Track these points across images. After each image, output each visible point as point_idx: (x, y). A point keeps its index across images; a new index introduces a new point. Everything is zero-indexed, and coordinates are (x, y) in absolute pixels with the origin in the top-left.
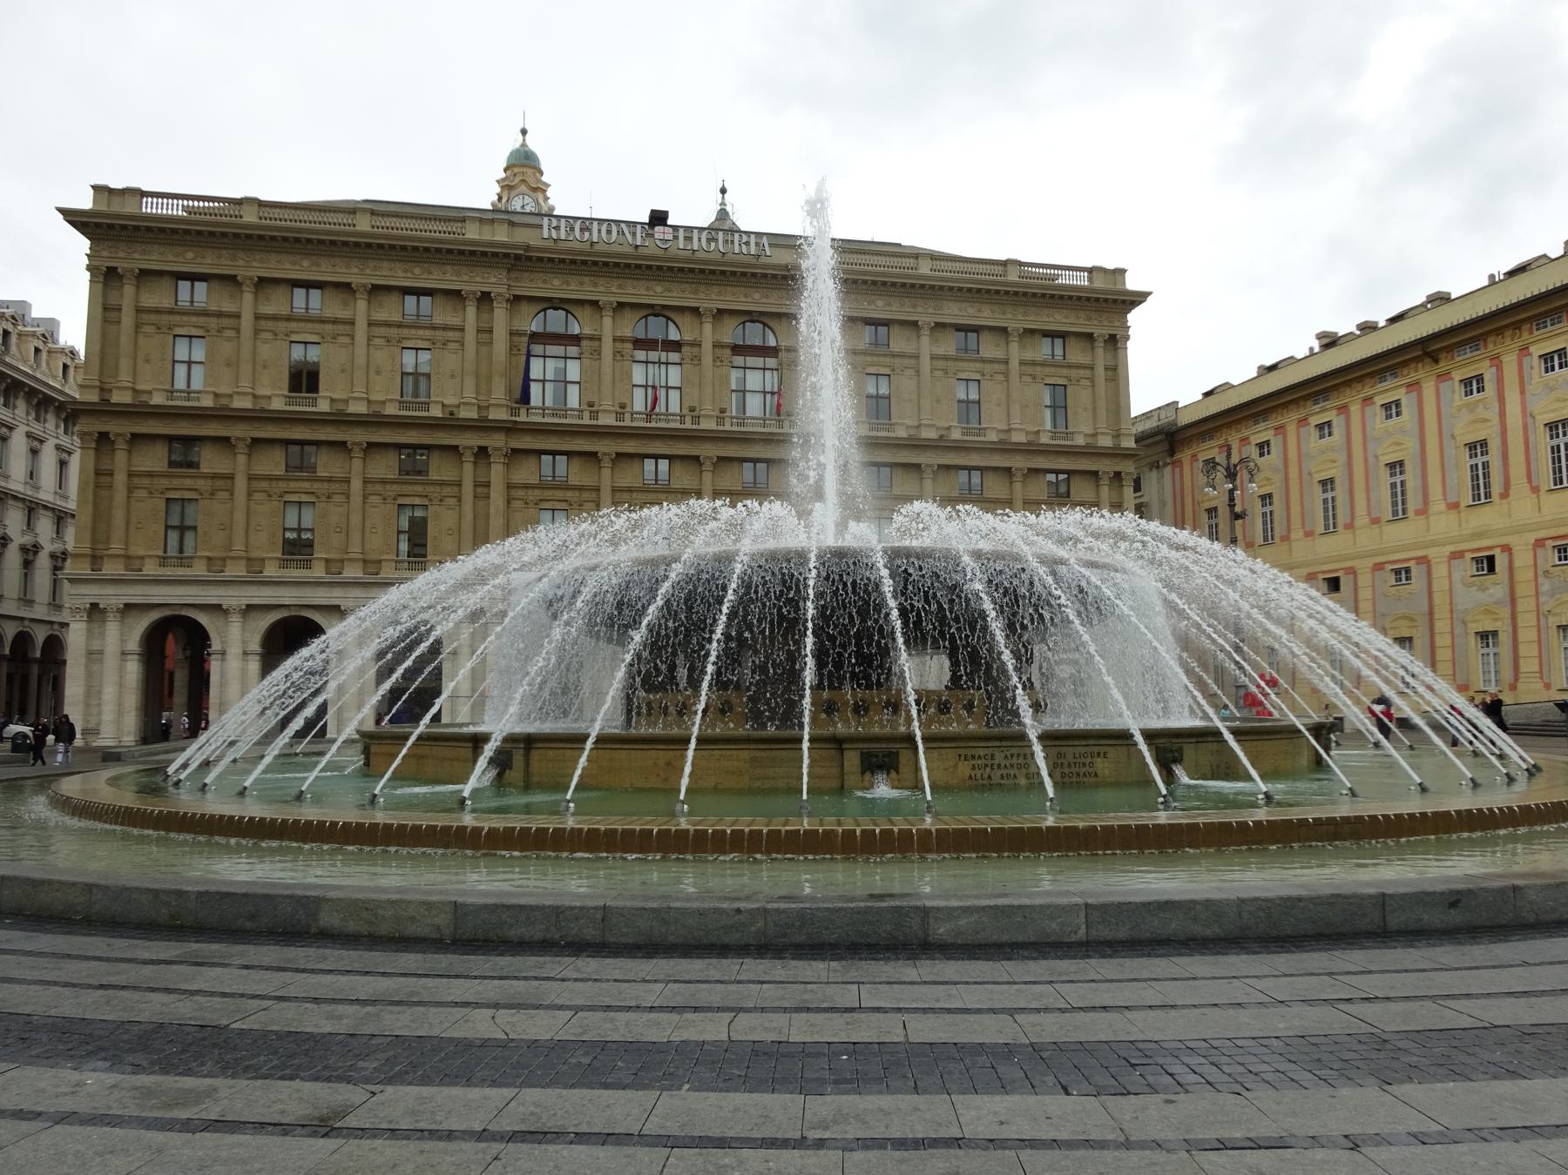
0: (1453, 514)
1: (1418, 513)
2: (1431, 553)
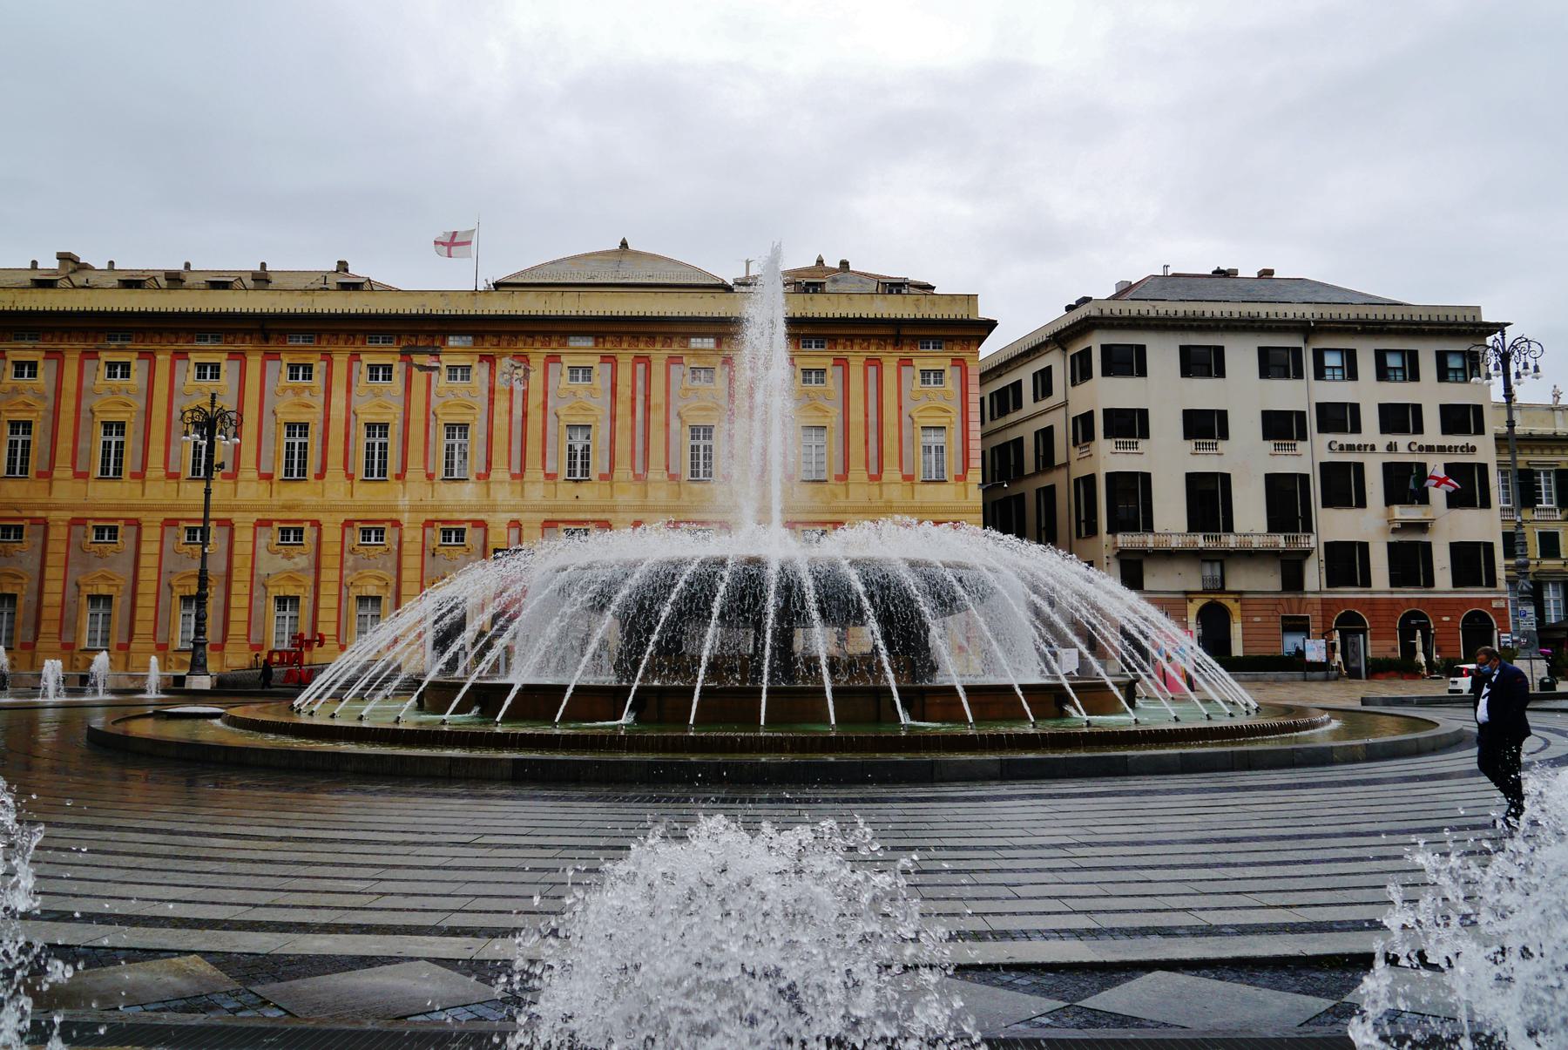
2: (236, 517)
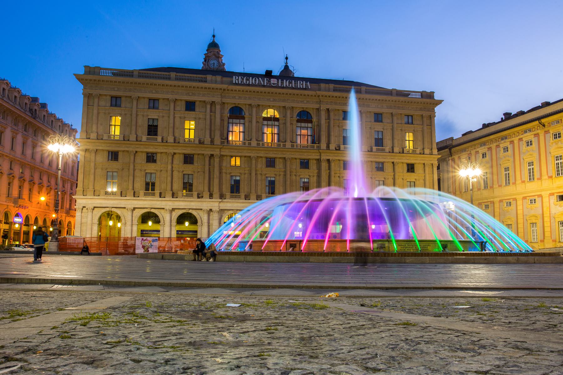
0: (550, 180)
1: (538, 179)
2: (543, 193)
